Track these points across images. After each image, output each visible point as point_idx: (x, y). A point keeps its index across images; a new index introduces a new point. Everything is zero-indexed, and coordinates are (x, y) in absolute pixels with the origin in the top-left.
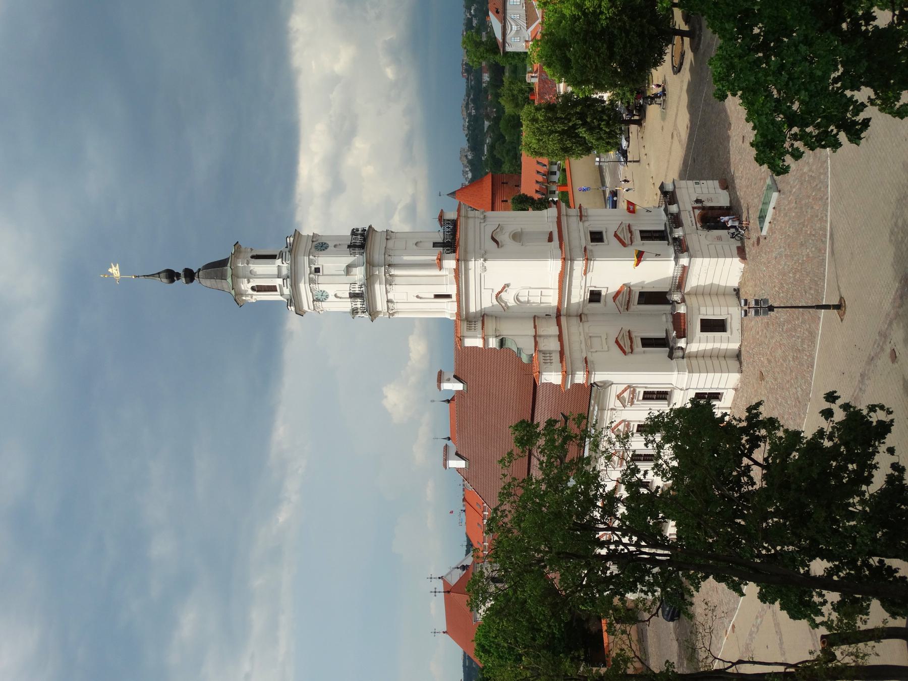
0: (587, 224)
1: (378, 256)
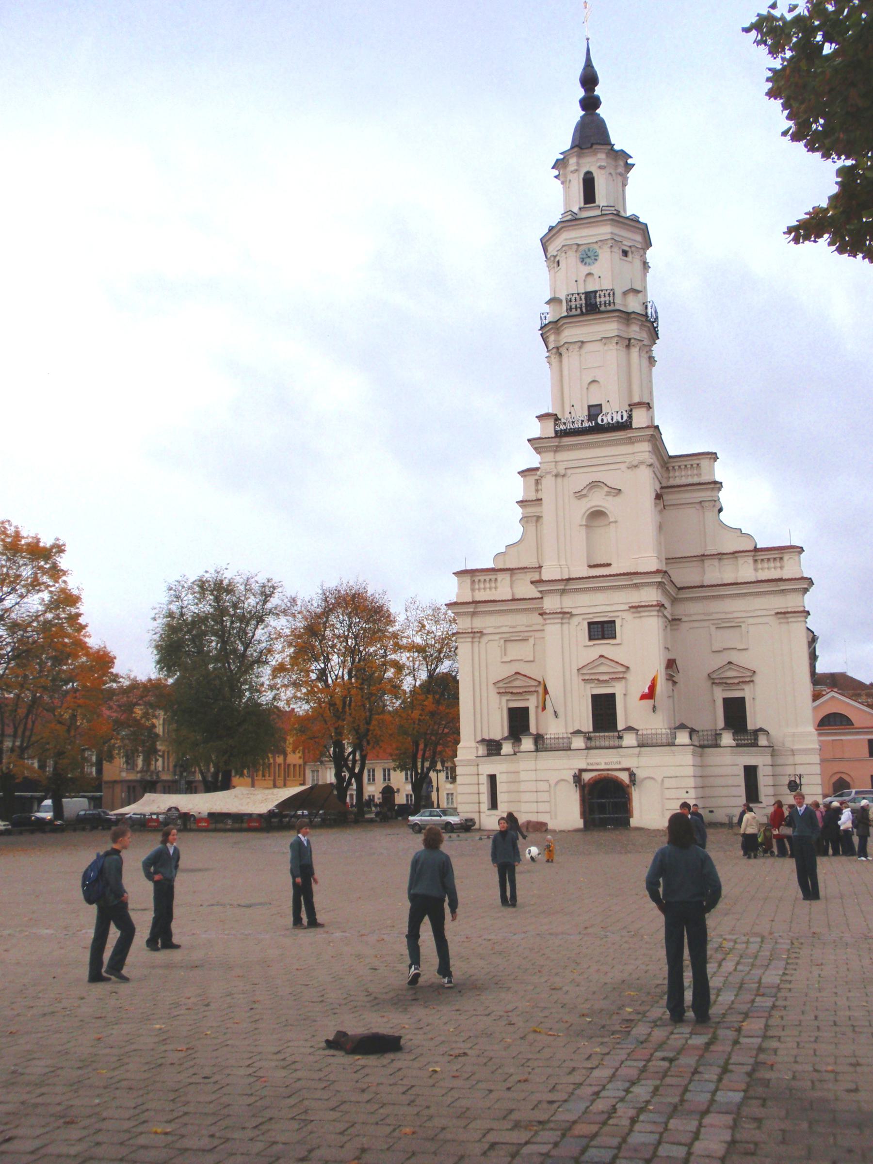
0: (628, 616)
1: (571, 333)
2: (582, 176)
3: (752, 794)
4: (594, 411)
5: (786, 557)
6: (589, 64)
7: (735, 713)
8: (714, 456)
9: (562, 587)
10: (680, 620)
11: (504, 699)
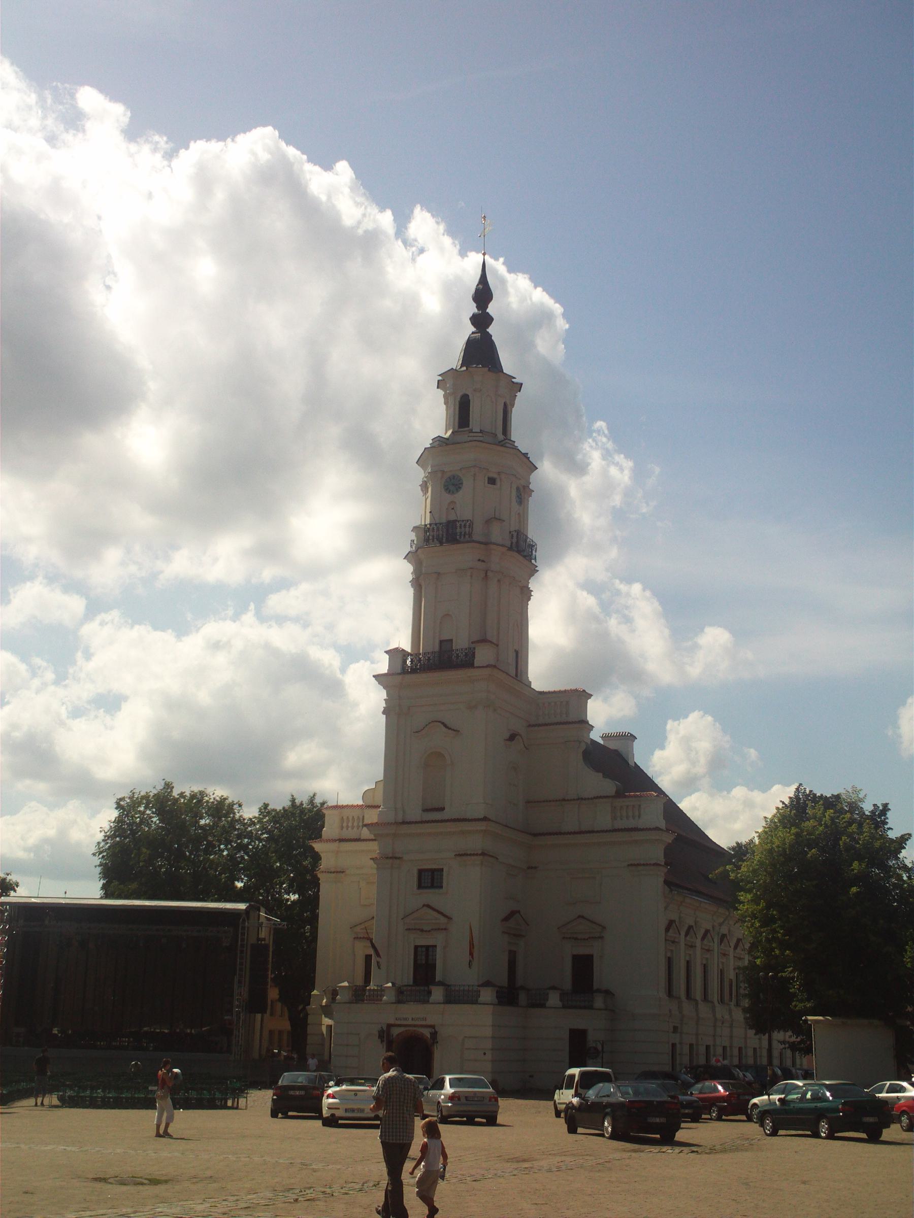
2: (458, 399)
4: (446, 644)
10: (535, 868)
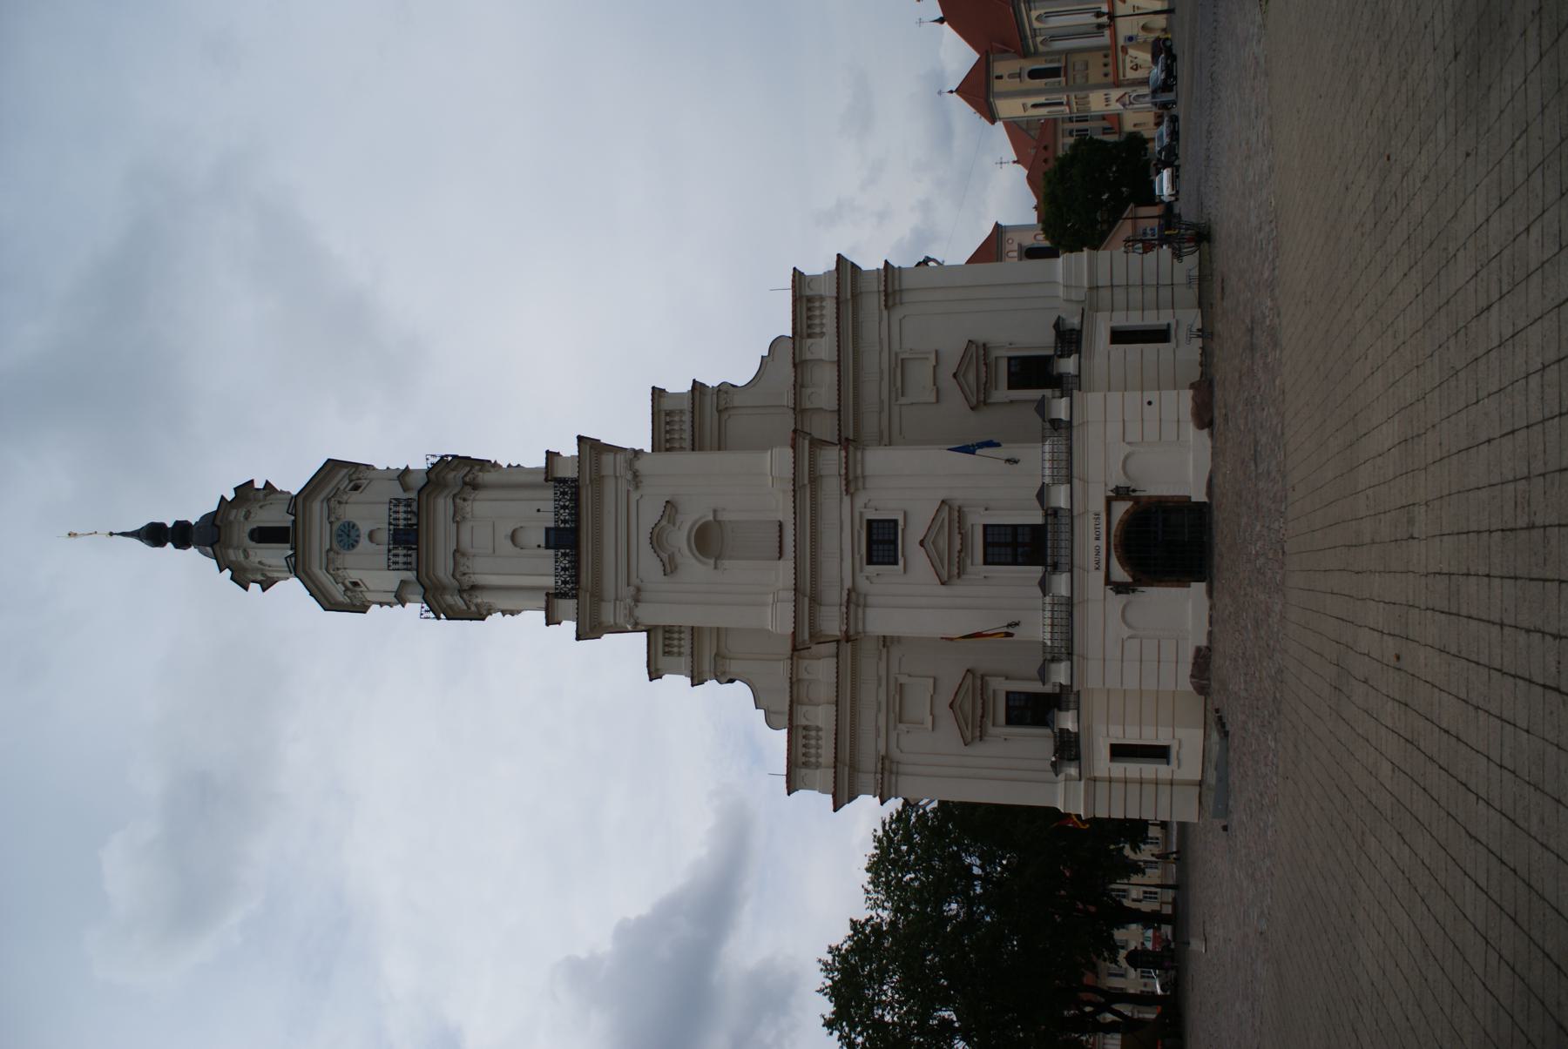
0: (861, 500)
1: (443, 569)
3: (1160, 335)
5: (808, 292)
6: (135, 534)
7: (1033, 372)
8: (657, 393)
9: (807, 600)
11: (991, 730)
